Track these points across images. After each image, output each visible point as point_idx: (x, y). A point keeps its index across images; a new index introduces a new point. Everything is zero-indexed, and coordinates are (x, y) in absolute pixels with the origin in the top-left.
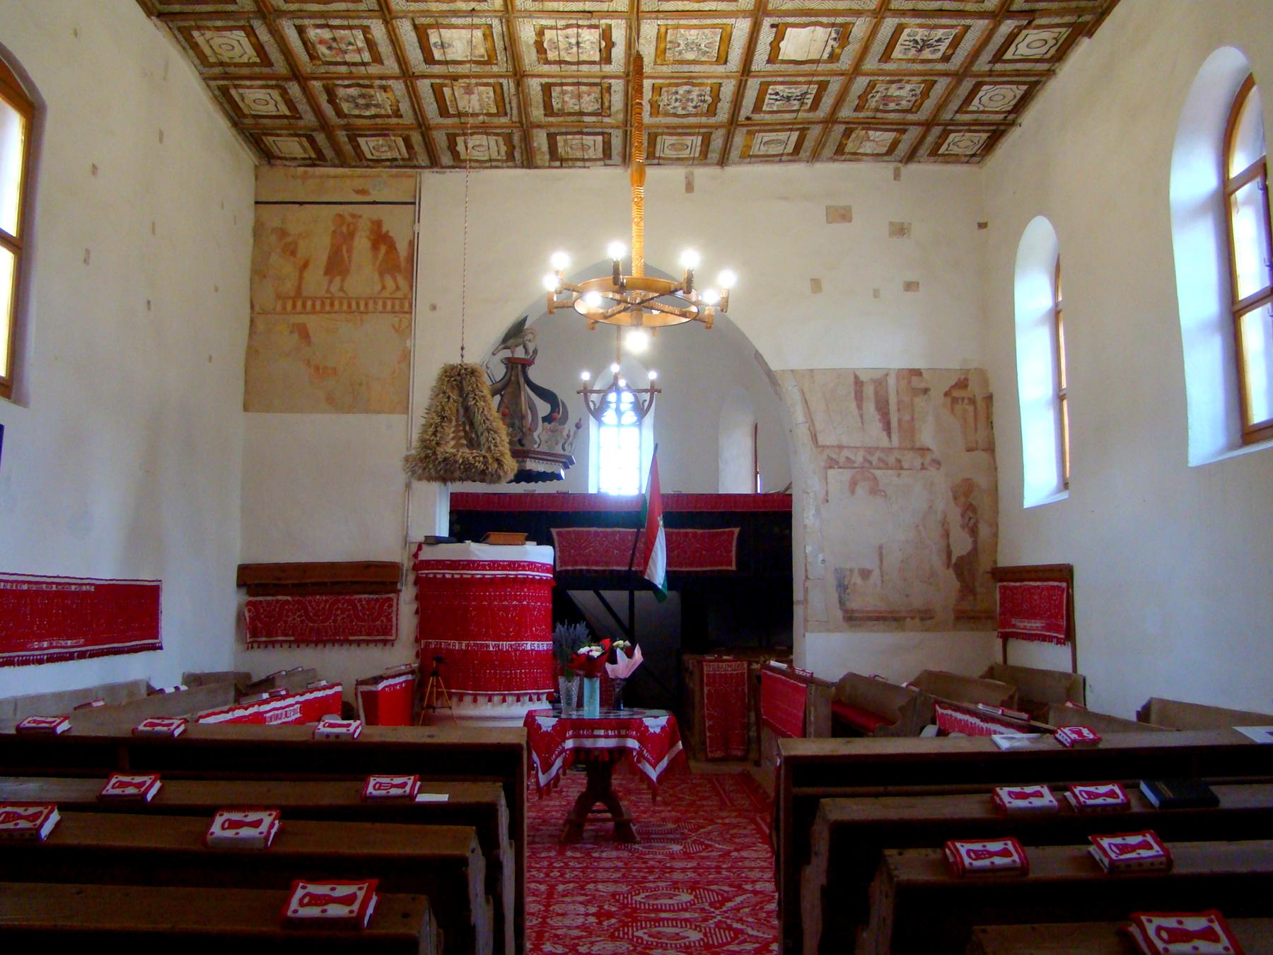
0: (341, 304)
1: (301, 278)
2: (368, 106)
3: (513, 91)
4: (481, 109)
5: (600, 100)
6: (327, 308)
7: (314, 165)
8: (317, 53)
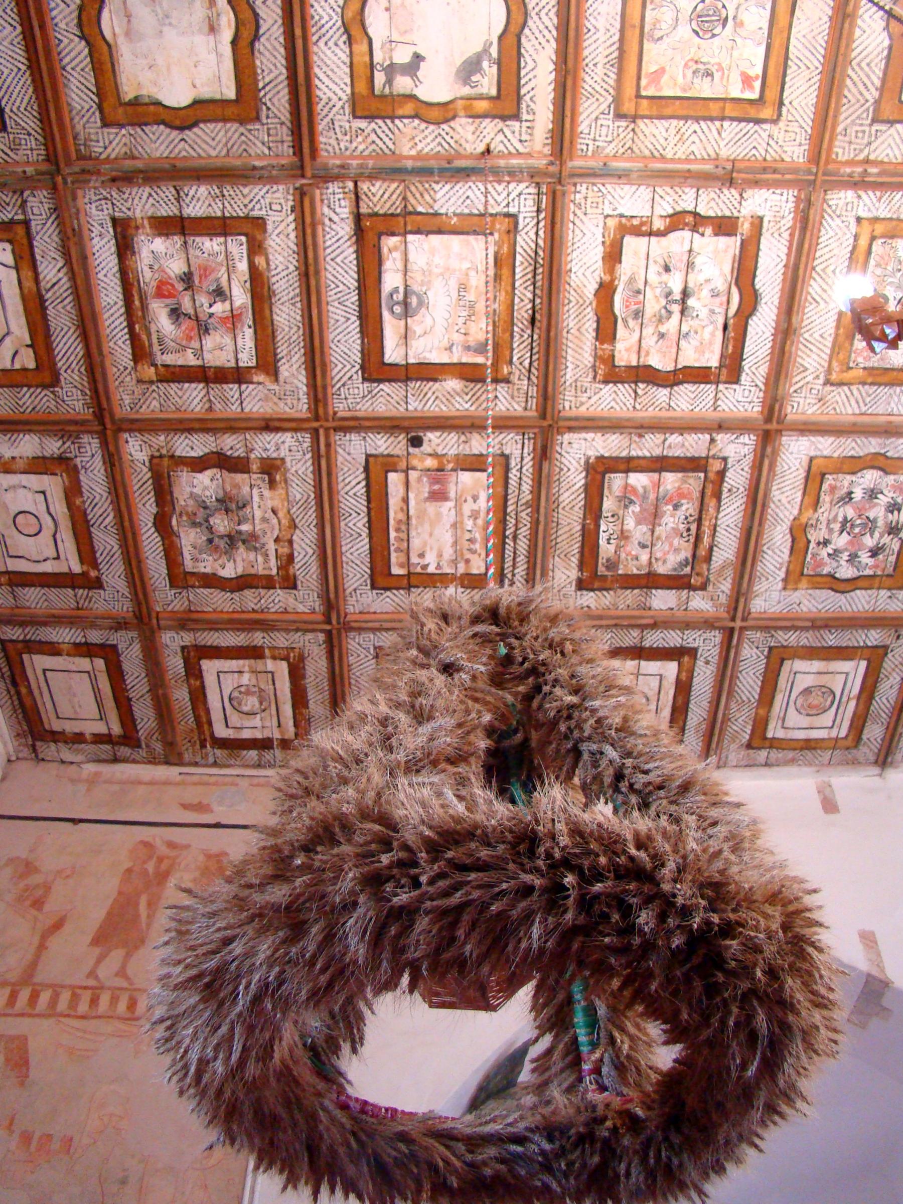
0: (114, 1000)
1: (42, 947)
2: (233, 540)
3: (526, 496)
4: (454, 562)
5: (694, 527)
6: (83, 1007)
7: (116, 760)
8: (149, 335)
